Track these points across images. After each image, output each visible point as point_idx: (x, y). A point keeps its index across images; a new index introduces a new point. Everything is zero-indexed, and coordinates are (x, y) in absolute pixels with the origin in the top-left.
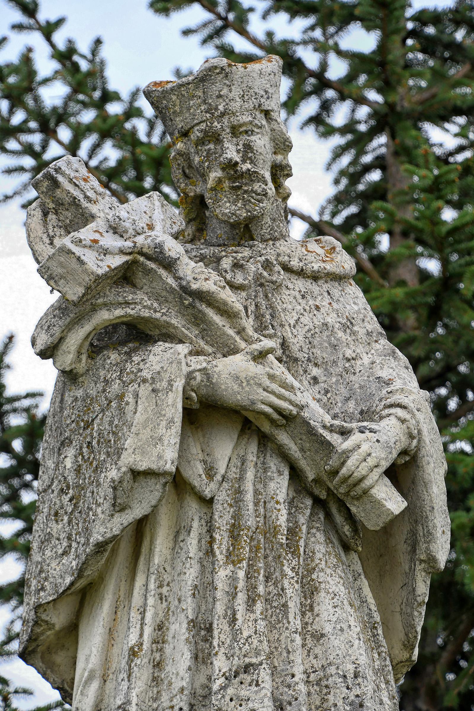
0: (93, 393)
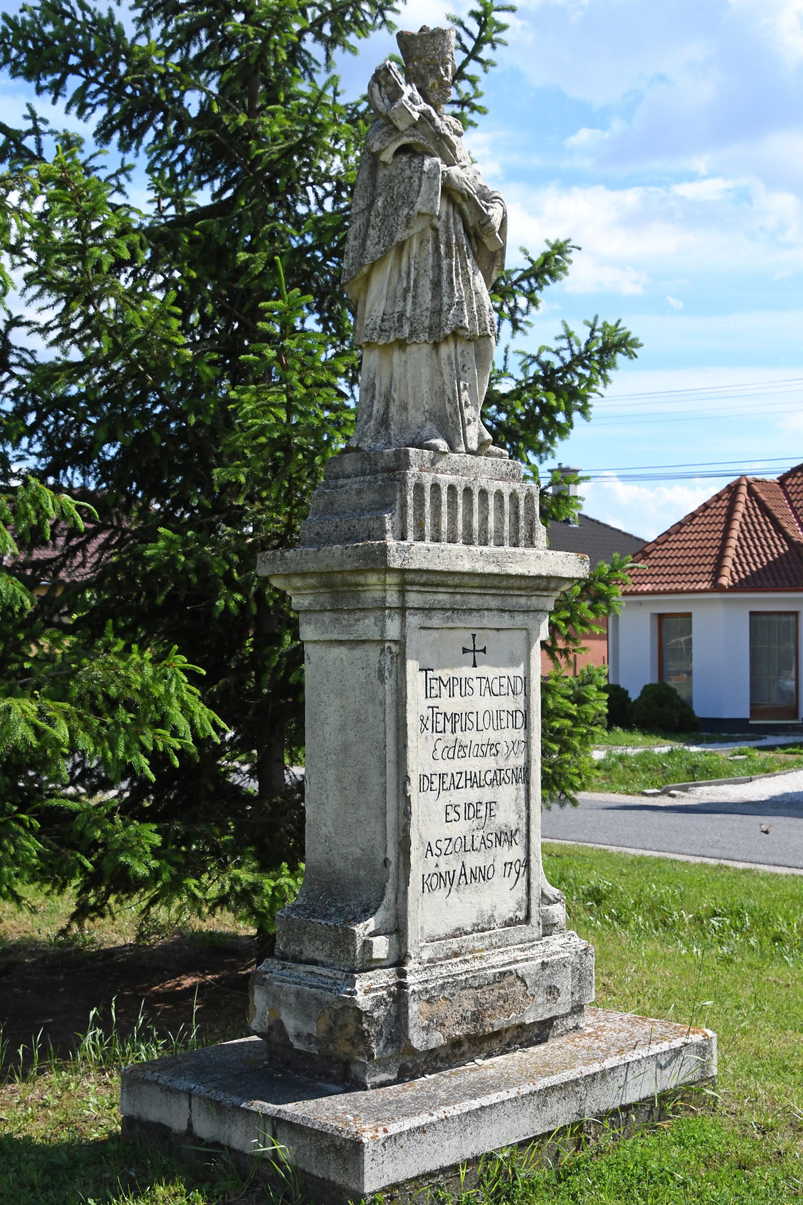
0: (394, 173)
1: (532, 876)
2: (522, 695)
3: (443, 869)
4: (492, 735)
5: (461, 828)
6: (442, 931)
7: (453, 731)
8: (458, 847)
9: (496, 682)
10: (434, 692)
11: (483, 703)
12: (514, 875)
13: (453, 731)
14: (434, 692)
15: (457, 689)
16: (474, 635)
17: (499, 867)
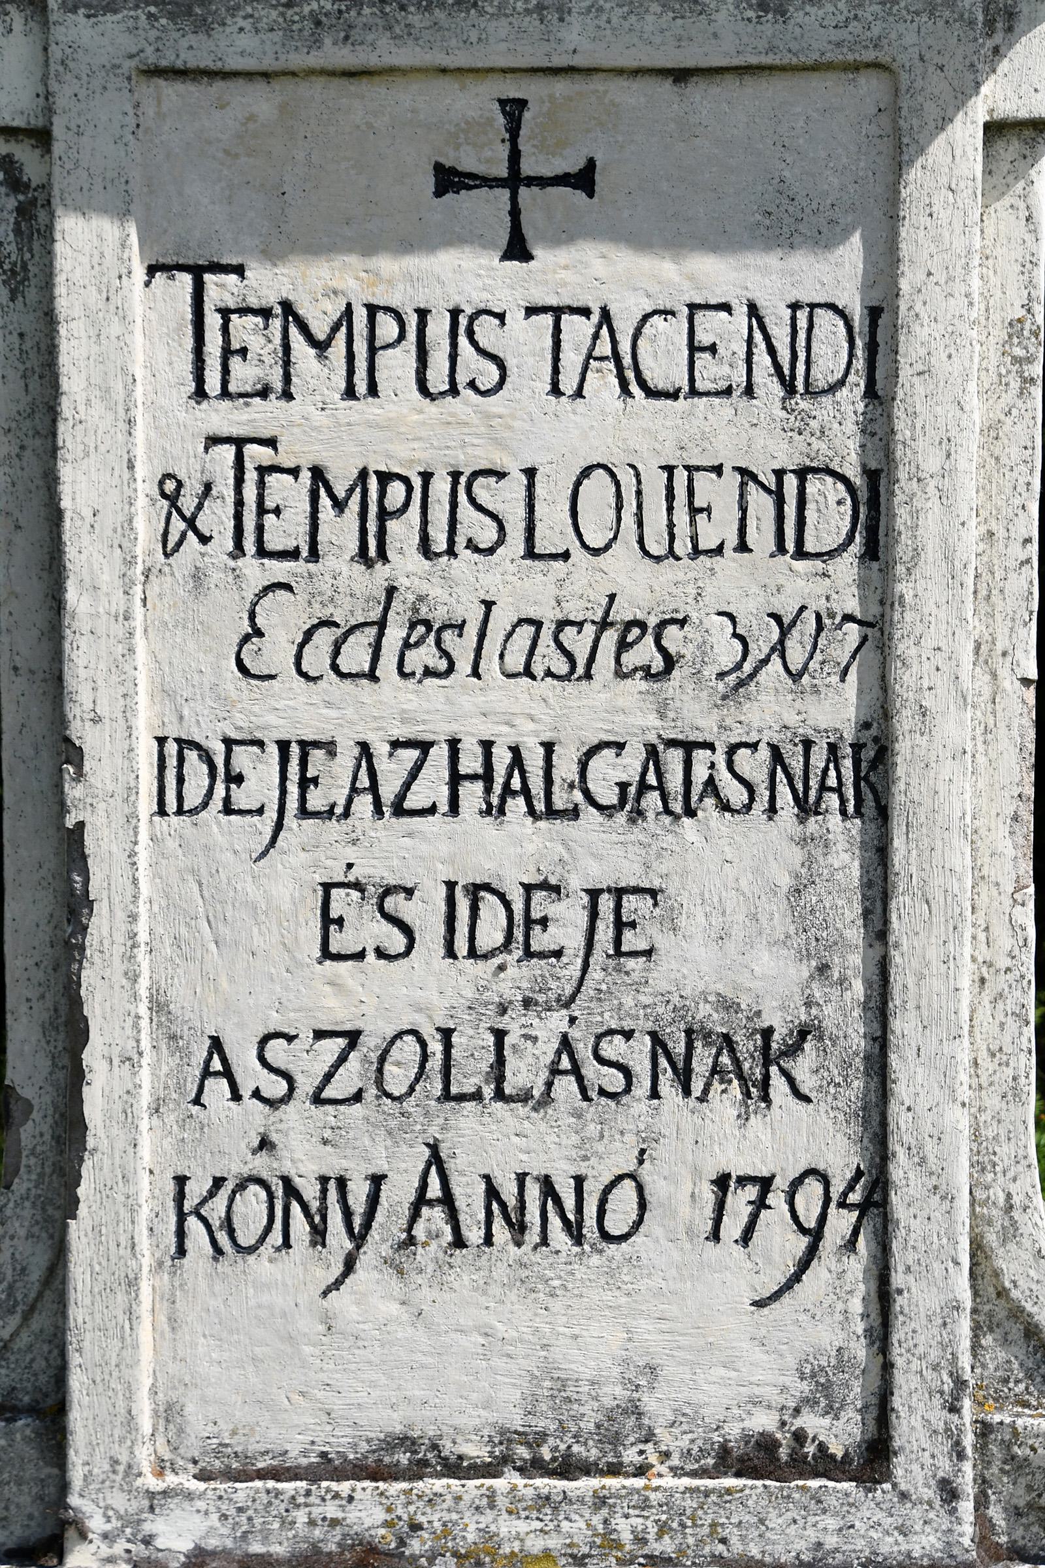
1: (900, 1256)
2: (852, 398)
3: (304, 1159)
4: (639, 587)
5: (427, 989)
6: (296, 1436)
7: (372, 552)
8: (397, 1078)
9: (667, 337)
10: (243, 374)
11: (548, 431)
12: (780, 1241)
13: (372, 552)
14: (243, 374)
15: (397, 365)
16: (513, 109)
17: (680, 1193)
